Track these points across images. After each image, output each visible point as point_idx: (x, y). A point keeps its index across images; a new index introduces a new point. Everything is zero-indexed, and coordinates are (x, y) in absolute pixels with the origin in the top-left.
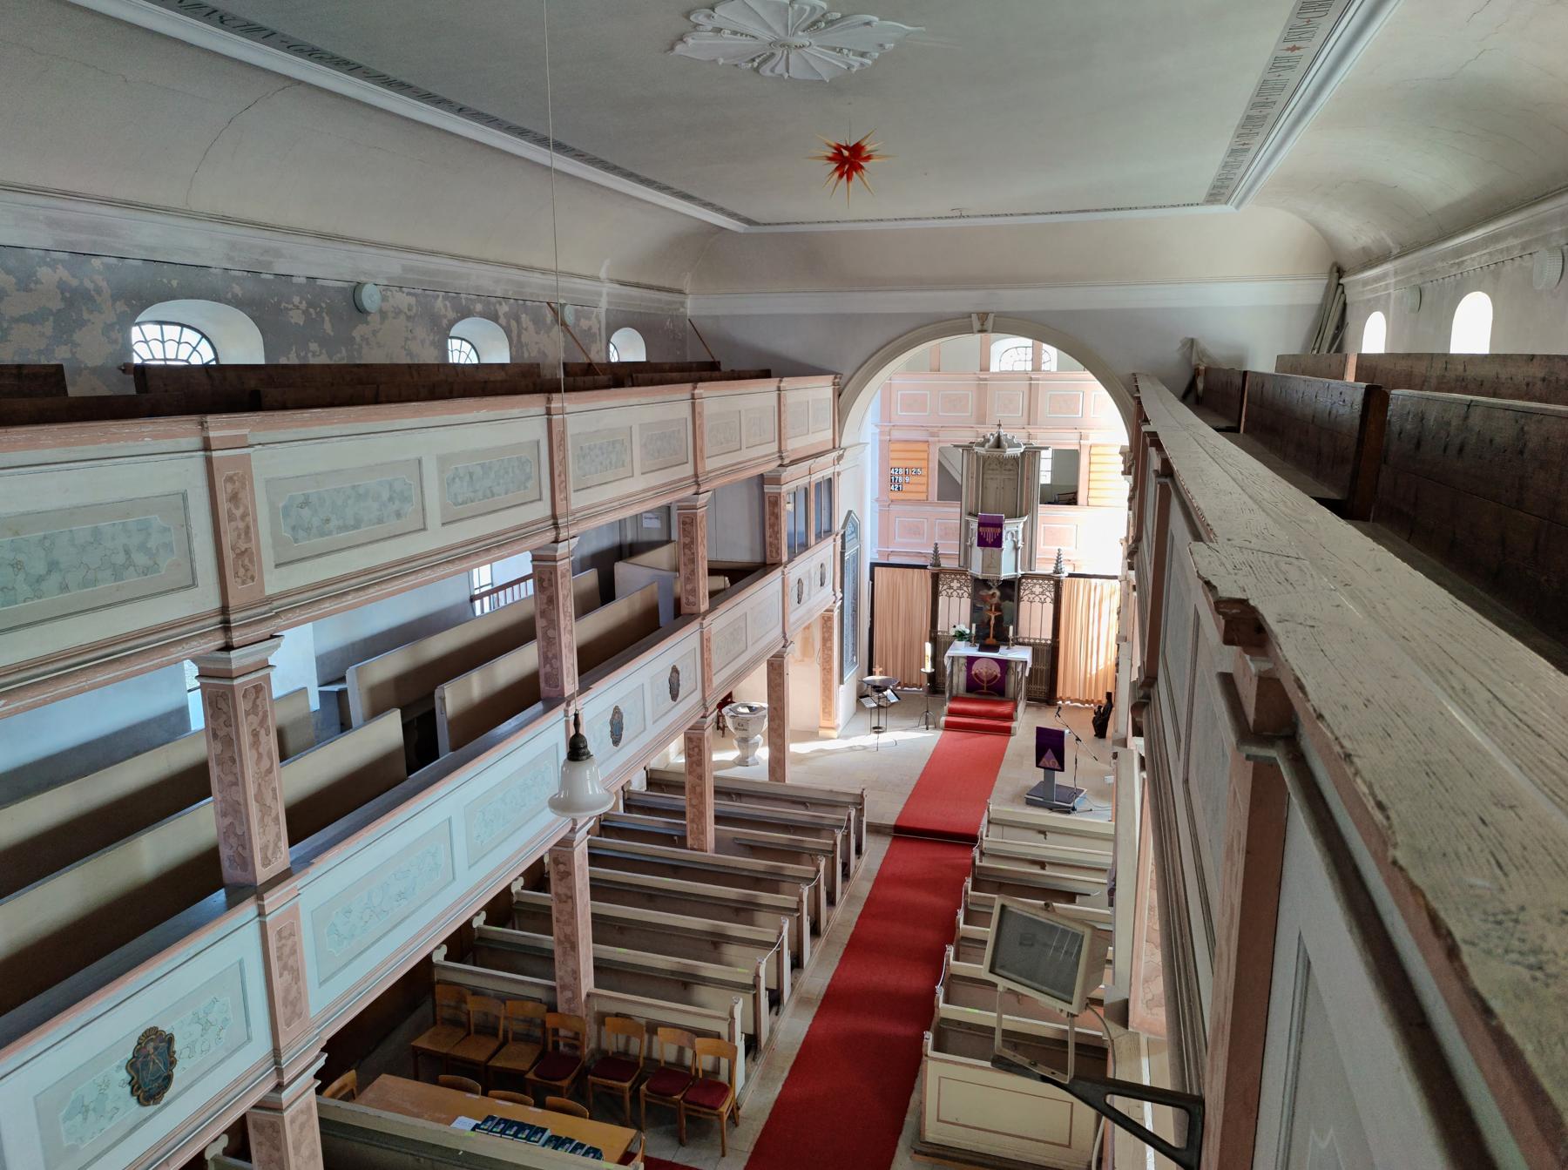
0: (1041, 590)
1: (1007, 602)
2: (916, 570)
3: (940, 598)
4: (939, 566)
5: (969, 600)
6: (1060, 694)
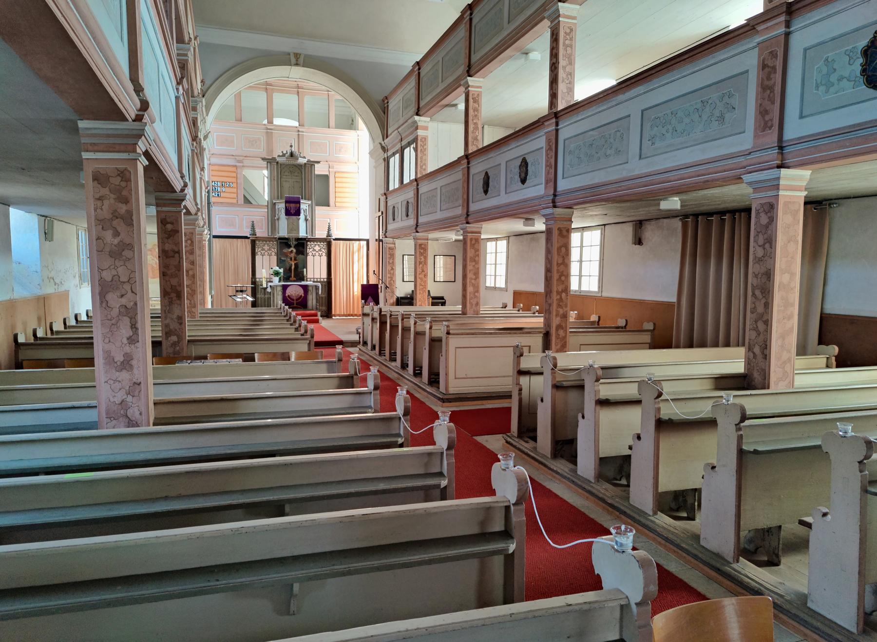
1: (300, 255)
2: (239, 240)
3: (257, 257)
4: (256, 235)
5: (275, 257)
6: (333, 313)
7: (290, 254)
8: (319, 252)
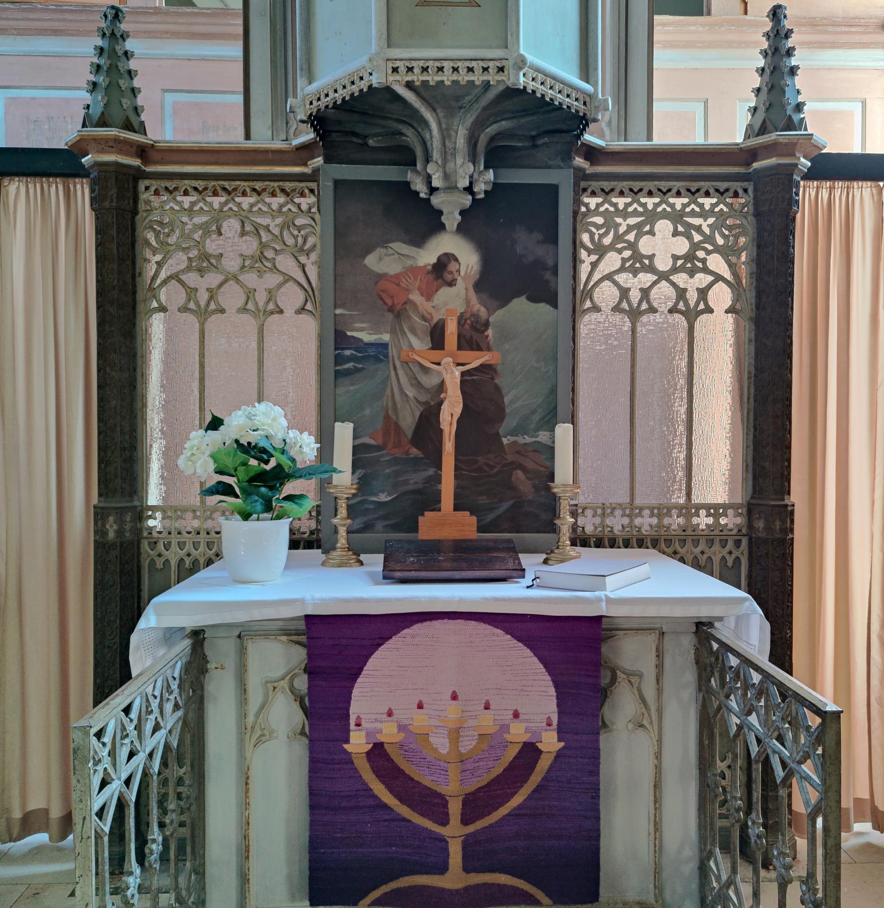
0: (682, 246)
1: (520, 304)
5: (310, 326)
7: (429, 297)
8: (681, 279)
